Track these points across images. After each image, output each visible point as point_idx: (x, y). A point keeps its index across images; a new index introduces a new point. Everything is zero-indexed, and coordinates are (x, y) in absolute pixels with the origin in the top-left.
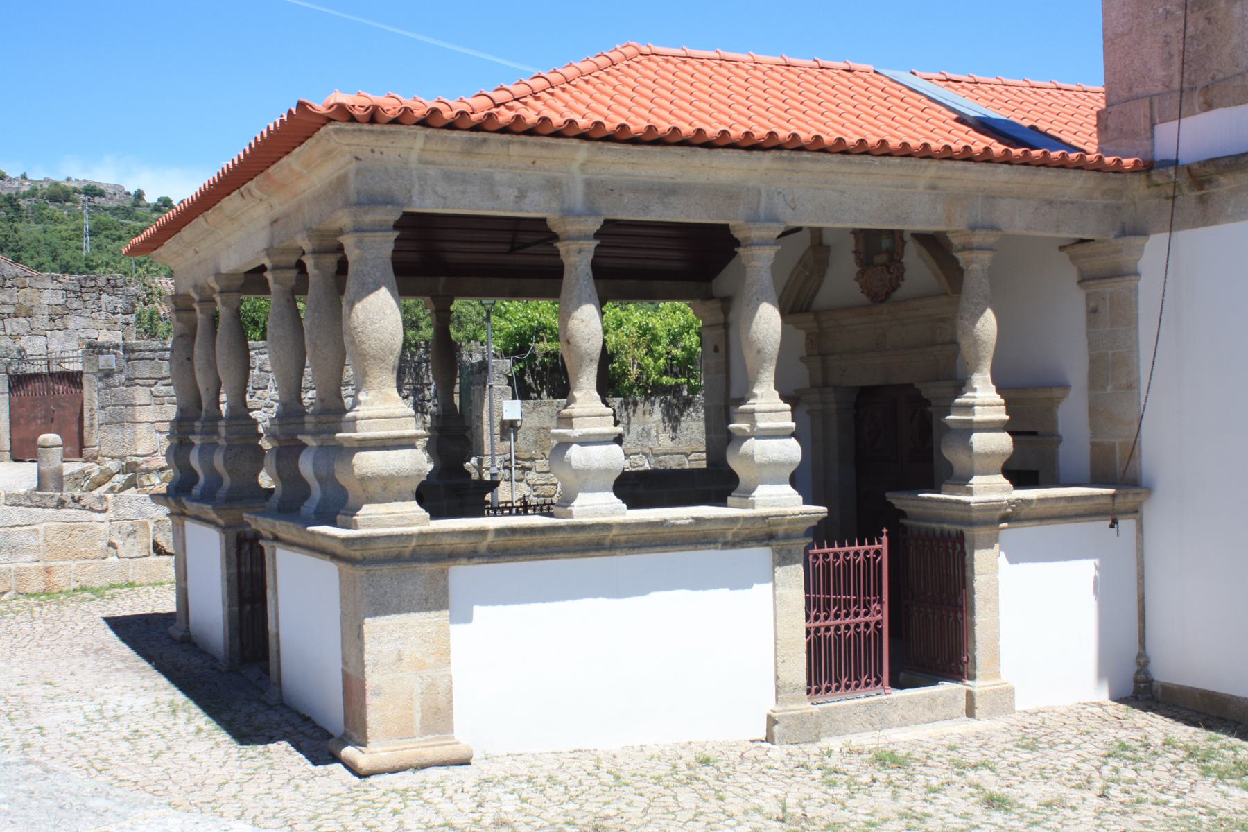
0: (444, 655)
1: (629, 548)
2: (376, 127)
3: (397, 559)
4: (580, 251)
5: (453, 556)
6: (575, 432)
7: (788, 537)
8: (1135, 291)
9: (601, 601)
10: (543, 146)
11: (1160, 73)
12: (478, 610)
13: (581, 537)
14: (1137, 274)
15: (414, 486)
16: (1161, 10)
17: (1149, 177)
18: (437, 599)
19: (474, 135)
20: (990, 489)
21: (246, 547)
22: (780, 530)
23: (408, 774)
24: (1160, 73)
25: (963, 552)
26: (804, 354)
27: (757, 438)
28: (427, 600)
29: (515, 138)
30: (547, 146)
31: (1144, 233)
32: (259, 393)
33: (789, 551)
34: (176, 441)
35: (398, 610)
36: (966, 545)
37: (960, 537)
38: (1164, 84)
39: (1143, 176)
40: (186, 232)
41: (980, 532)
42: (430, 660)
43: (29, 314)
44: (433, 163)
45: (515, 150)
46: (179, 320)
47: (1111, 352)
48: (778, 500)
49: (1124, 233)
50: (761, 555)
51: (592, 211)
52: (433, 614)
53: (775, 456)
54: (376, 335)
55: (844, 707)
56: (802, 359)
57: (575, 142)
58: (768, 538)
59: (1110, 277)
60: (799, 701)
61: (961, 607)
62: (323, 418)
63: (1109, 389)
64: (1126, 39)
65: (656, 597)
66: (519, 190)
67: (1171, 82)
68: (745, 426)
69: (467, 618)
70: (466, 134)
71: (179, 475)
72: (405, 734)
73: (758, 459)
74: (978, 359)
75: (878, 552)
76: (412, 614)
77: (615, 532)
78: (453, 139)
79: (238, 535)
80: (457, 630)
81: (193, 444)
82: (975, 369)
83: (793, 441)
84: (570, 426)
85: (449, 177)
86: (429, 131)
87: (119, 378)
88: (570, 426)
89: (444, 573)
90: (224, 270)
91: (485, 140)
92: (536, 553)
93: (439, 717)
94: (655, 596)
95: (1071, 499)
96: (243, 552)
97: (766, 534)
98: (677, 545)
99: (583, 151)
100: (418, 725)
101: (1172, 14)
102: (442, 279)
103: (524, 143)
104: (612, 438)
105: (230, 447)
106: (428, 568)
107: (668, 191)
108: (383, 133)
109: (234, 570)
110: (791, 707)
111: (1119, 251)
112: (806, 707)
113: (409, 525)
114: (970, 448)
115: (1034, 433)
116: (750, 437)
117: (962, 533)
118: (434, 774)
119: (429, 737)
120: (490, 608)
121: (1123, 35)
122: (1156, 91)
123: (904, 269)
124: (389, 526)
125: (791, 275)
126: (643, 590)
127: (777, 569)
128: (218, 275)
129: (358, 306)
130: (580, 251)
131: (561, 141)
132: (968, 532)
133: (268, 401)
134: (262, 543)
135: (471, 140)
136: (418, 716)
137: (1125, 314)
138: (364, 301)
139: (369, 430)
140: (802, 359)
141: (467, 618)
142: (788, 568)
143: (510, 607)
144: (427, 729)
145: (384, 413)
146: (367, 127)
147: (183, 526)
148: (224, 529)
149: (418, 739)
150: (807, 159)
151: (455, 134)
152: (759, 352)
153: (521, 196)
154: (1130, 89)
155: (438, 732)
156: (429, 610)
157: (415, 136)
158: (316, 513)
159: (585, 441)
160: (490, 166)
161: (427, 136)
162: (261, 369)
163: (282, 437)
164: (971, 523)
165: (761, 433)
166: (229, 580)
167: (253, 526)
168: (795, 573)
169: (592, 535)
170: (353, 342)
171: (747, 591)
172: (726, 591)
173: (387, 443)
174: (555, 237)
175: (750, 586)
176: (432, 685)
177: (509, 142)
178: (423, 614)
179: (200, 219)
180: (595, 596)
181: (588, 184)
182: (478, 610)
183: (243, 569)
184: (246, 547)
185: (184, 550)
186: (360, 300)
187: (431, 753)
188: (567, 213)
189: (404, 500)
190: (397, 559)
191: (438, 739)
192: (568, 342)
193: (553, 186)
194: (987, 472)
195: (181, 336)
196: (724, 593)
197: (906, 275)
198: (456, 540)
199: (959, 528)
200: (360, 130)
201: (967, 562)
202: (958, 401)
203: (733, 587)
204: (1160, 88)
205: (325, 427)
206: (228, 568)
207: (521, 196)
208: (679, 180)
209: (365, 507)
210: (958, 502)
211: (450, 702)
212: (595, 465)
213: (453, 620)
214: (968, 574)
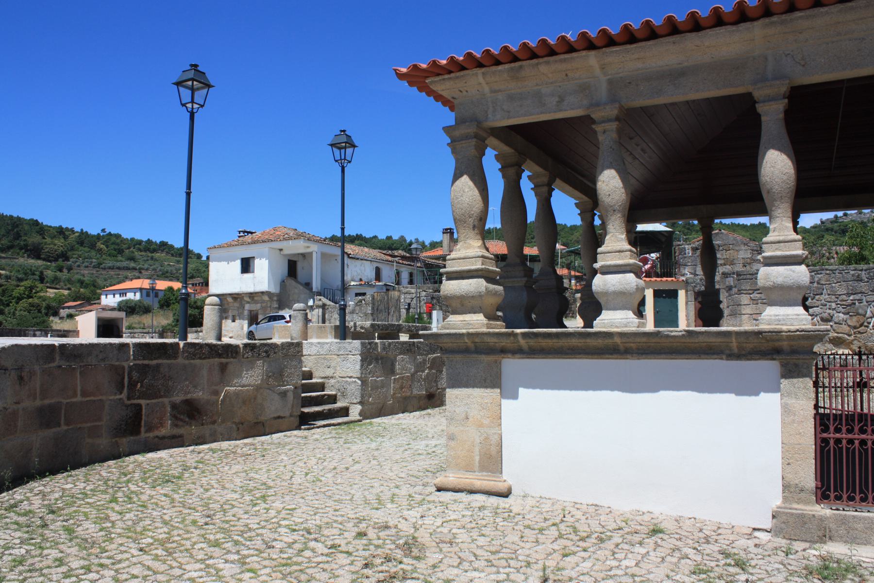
0: (498, 418)
1: (638, 354)
3: (466, 351)
4: (604, 132)
5: (504, 351)
7: (794, 352)
9: (617, 394)
10: (561, 61)
12: (522, 391)
18: (492, 380)
19: (513, 65)
22: (785, 344)
23: (450, 494)
28: (485, 380)
29: (541, 60)
30: (565, 60)
32: (817, 297)
33: (796, 365)
35: (467, 386)
42: (486, 422)
43: (732, 263)
44: (500, 91)
45: (543, 68)
50: (771, 366)
51: (613, 99)
52: (489, 390)
53: (780, 280)
54: (458, 206)
55: (865, 518)
57: (584, 53)
60: (806, 502)
65: (665, 395)
66: (560, 97)
69: (515, 396)
70: (507, 66)
72: (469, 469)
76: (476, 389)
78: (500, 71)
80: (507, 404)
85: (511, 98)
86: (483, 70)
87: (735, 290)
91: (521, 67)
93: (492, 461)
94: (662, 393)
99: (592, 59)
100: (477, 464)
103: (548, 63)
107: (676, 75)
108: (457, 78)
110: (795, 506)
112: (823, 511)
118: (480, 498)
119: (485, 473)
120: (531, 390)
127: (782, 380)
130: (604, 132)
131: (574, 55)
133: (823, 302)
135: (512, 69)
136: (477, 458)
141: (515, 396)
142: (795, 380)
143: (545, 391)
144: (483, 468)
145: (462, 256)
149: (477, 473)
150: (801, 17)
151: (500, 67)
152: (768, 192)
153: (561, 100)
155: (490, 471)
156: (486, 387)
157: (476, 75)
159: (608, 270)
160: (537, 85)
161: (483, 73)
162: (818, 283)
169: (608, 341)
171: (753, 398)
172: (733, 395)
175: (757, 394)
176: (486, 438)
177: (537, 64)
178: (482, 390)
180: (612, 389)
181: (610, 82)
182: (522, 391)
187: (478, 484)
188: (598, 105)
190: (466, 351)
191: (490, 476)
193: (584, 88)
198: (494, 340)
200: (444, 79)
201: (703, 356)
203: (737, 395)
207: (561, 100)
208: (686, 64)
211: (501, 452)
212: (612, 289)
213: (503, 395)
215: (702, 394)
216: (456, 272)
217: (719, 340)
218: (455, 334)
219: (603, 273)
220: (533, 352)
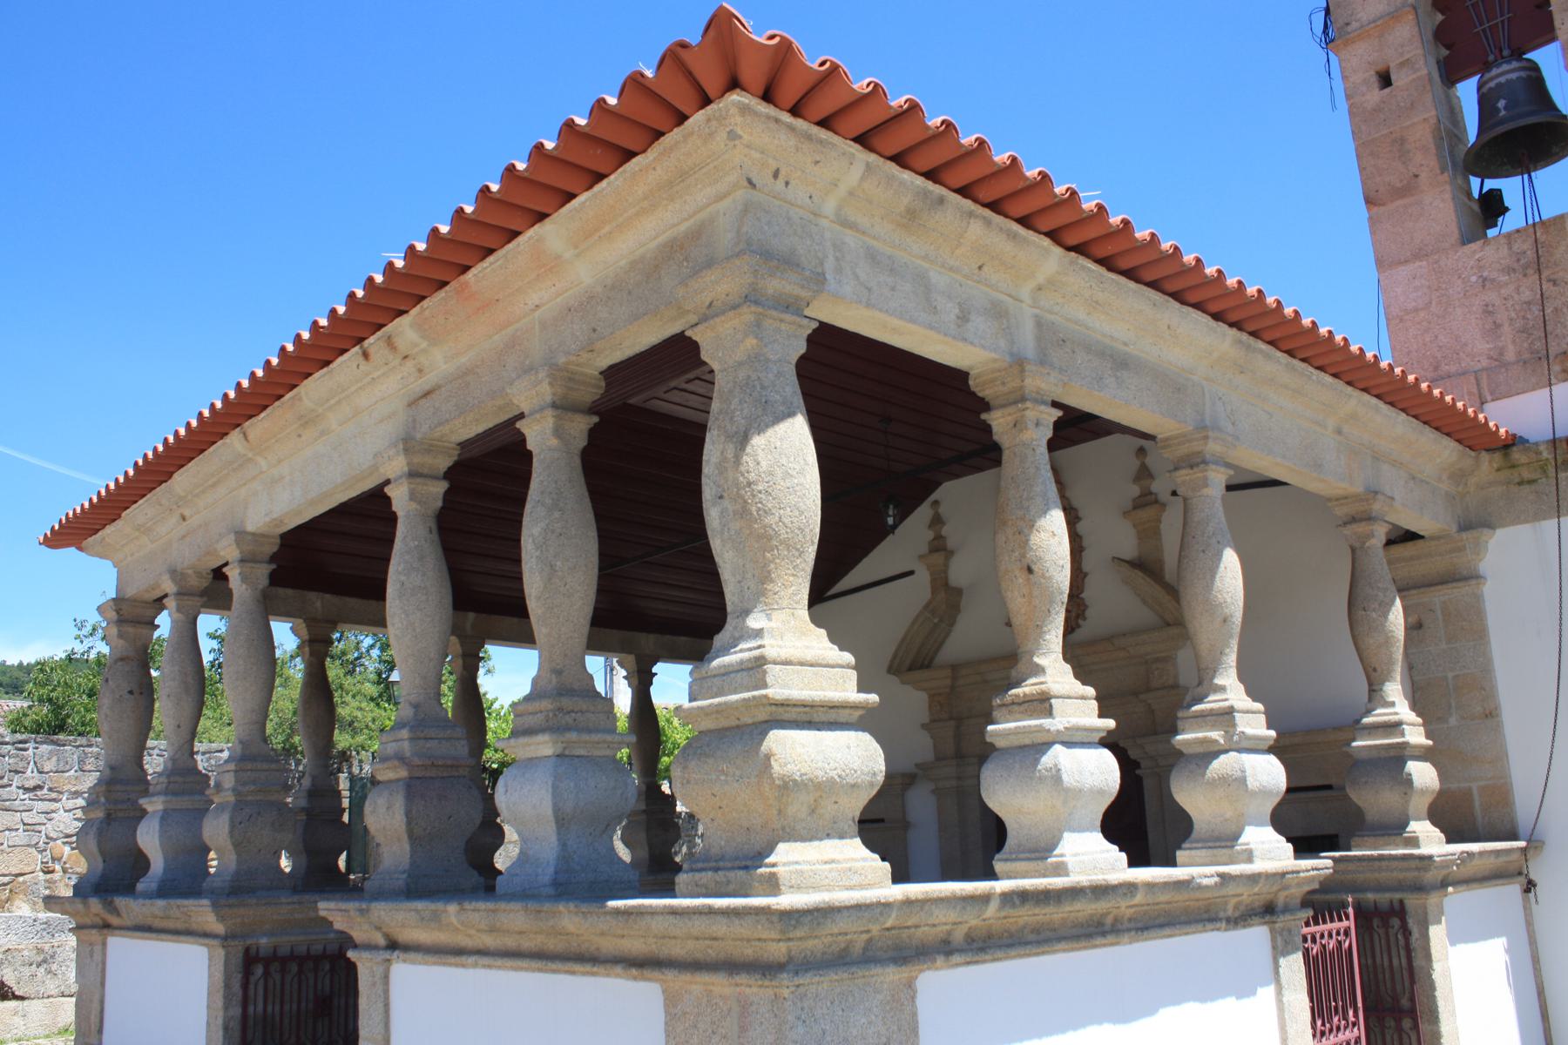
1: (1137, 930)
2: (799, 123)
6: (1056, 723)
8: (1478, 598)
11: (1483, 346)
13: (1084, 909)
14: (1474, 577)
15: (855, 805)
16: (1474, 279)
17: (1506, 455)
19: (930, 185)
20: (1429, 840)
21: (259, 970)
24: (1483, 346)
25: (1407, 933)
26: (927, 720)
27: (1239, 751)
31: (1491, 526)
34: (99, 814)
36: (1412, 923)
37: (1400, 911)
38: (1490, 358)
39: (1497, 456)
40: (182, 480)
41: (1432, 899)
45: (976, 229)
46: (120, 636)
47: (1450, 675)
48: (1268, 850)
49: (1466, 526)
50: (1257, 936)
54: (793, 499)
56: (924, 726)
58: (1268, 911)
59: (1442, 583)
61: (1412, 1013)
62: (566, 702)
63: (1453, 721)
64: (1422, 314)
67: (1501, 354)
68: (1216, 735)
71: (100, 865)
73: (1252, 784)
74: (1391, 662)
75: (1347, 933)
77: (1139, 898)
78: (902, 183)
79: (247, 950)
81: (144, 812)
82: (1387, 677)
83: (1272, 759)
84: (1049, 713)
85: (872, 257)
88: (1049, 713)
89: (910, 985)
90: (250, 528)
91: (941, 200)
92: (1027, 943)
94: (1167, 1014)
95: (1497, 853)
96: (253, 979)
97: (1264, 907)
98: (1161, 926)
101: (1493, 280)
102: (471, 615)
104: (1096, 737)
105: (240, 805)
106: (891, 975)
108: (809, 137)
109: (237, 1011)
111: (1461, 549)
113: (862, 887)
114: (1408, 781)
115: (1329, 787)
116: (1226, 751)
117: (1401, 902)
121: (1416, 310)
122: (1479, 366)
123: (1086, 607)
124: (829, 888)
125: (913, 623)
126: (1151, 1011)
127: (1282, 961)
128: (240, 535)
129: (758, 441)
132: (1412, 901)
134: (351, 954)
135: (926, 194)
137: (1470, 627)
138: (770, 432)
139: (785, 686)
140: (924, 726)
146: (786, 117)
147: (104, 944)
148: (225, 939)
150: (1261, 351)
152: (1225, 621)
154: (1436, 368)
158: (555, 883)
160: (925, 258)
163: (417, 761)
164: (1420, 888)
165: (1245, 744)
166: (226, 1028)
167: (337, 926)
168: (1294, 967)
170: (744, 512)
172: (1231, 1000)
173: (820, 716)
174: (985, 406)
175: (1254, 993)
177: (971, 214)
179: (234, 438)
180: (1100, 1023)
183: (251, 1009)
184: (259, 970)
185: (103, 984)
186: (760, 431)
189: (841, 837)
192: (1030, 570)
194: (1418, 819)
195: (122, 659)
196: (1191, 1007)
197: (1088, 613)
199: (1397, 896)
200: (777, 121)
202: (1366, 720)
203: (1239, 996)
204: (1485, 363)
205: (569, 719)
206: (226, 1008)
209: (781, 847)
210: (1381, 858)
214: (1418, 962)
215: (1209, 1005)
216: (804, 705)
217: (1178, 897)
218: (859, 907)
219: (1069, 744)
220: (982, 945)
